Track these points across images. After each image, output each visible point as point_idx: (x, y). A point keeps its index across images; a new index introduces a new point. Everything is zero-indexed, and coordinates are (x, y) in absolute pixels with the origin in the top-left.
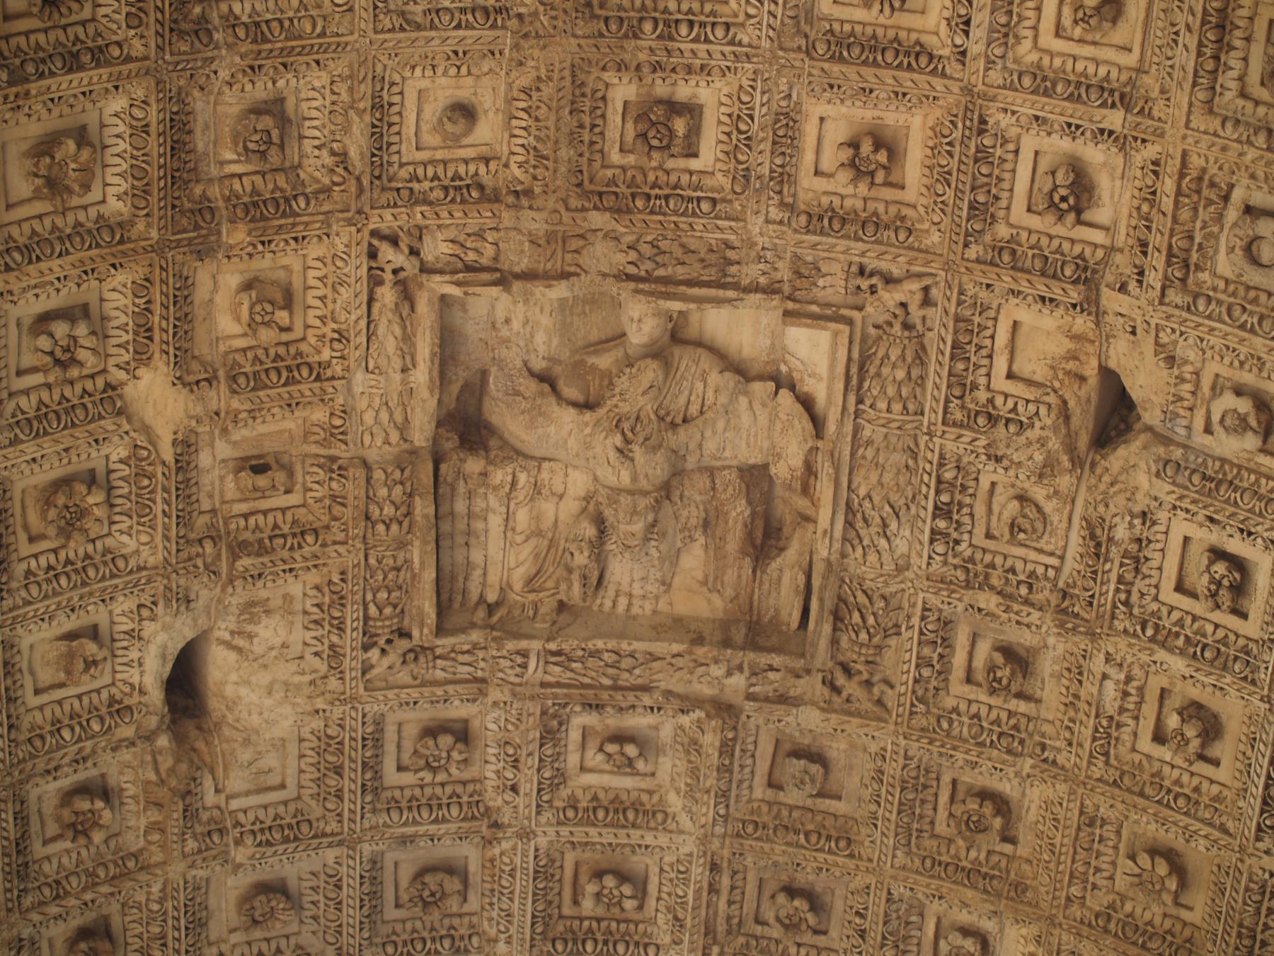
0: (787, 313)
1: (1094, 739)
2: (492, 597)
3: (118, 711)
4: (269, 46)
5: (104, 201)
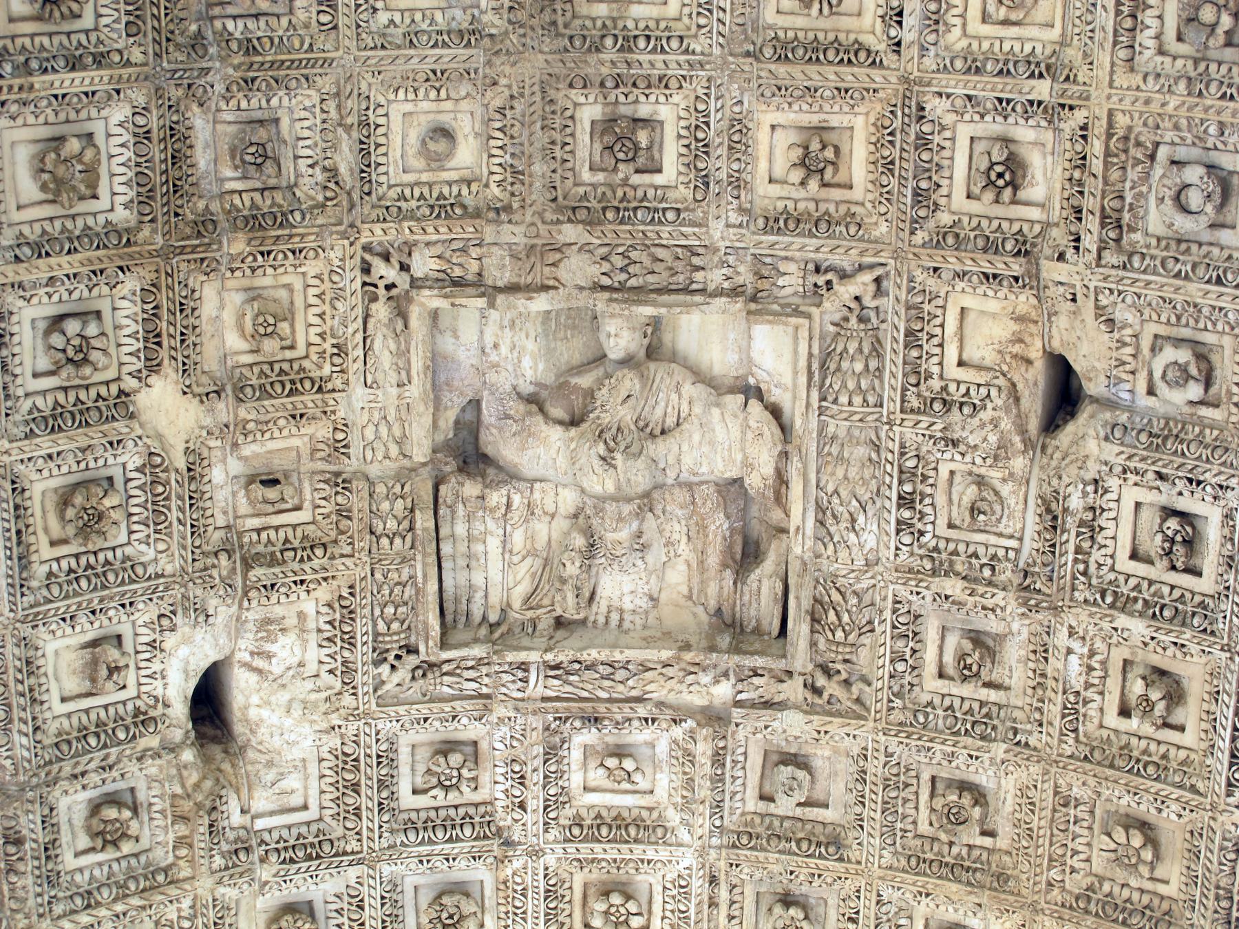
0: (749, 313)
1: (1063, 716)
2: (493, 617)
3: (143, 722)
4: (259, 59)
5: (112, 210)
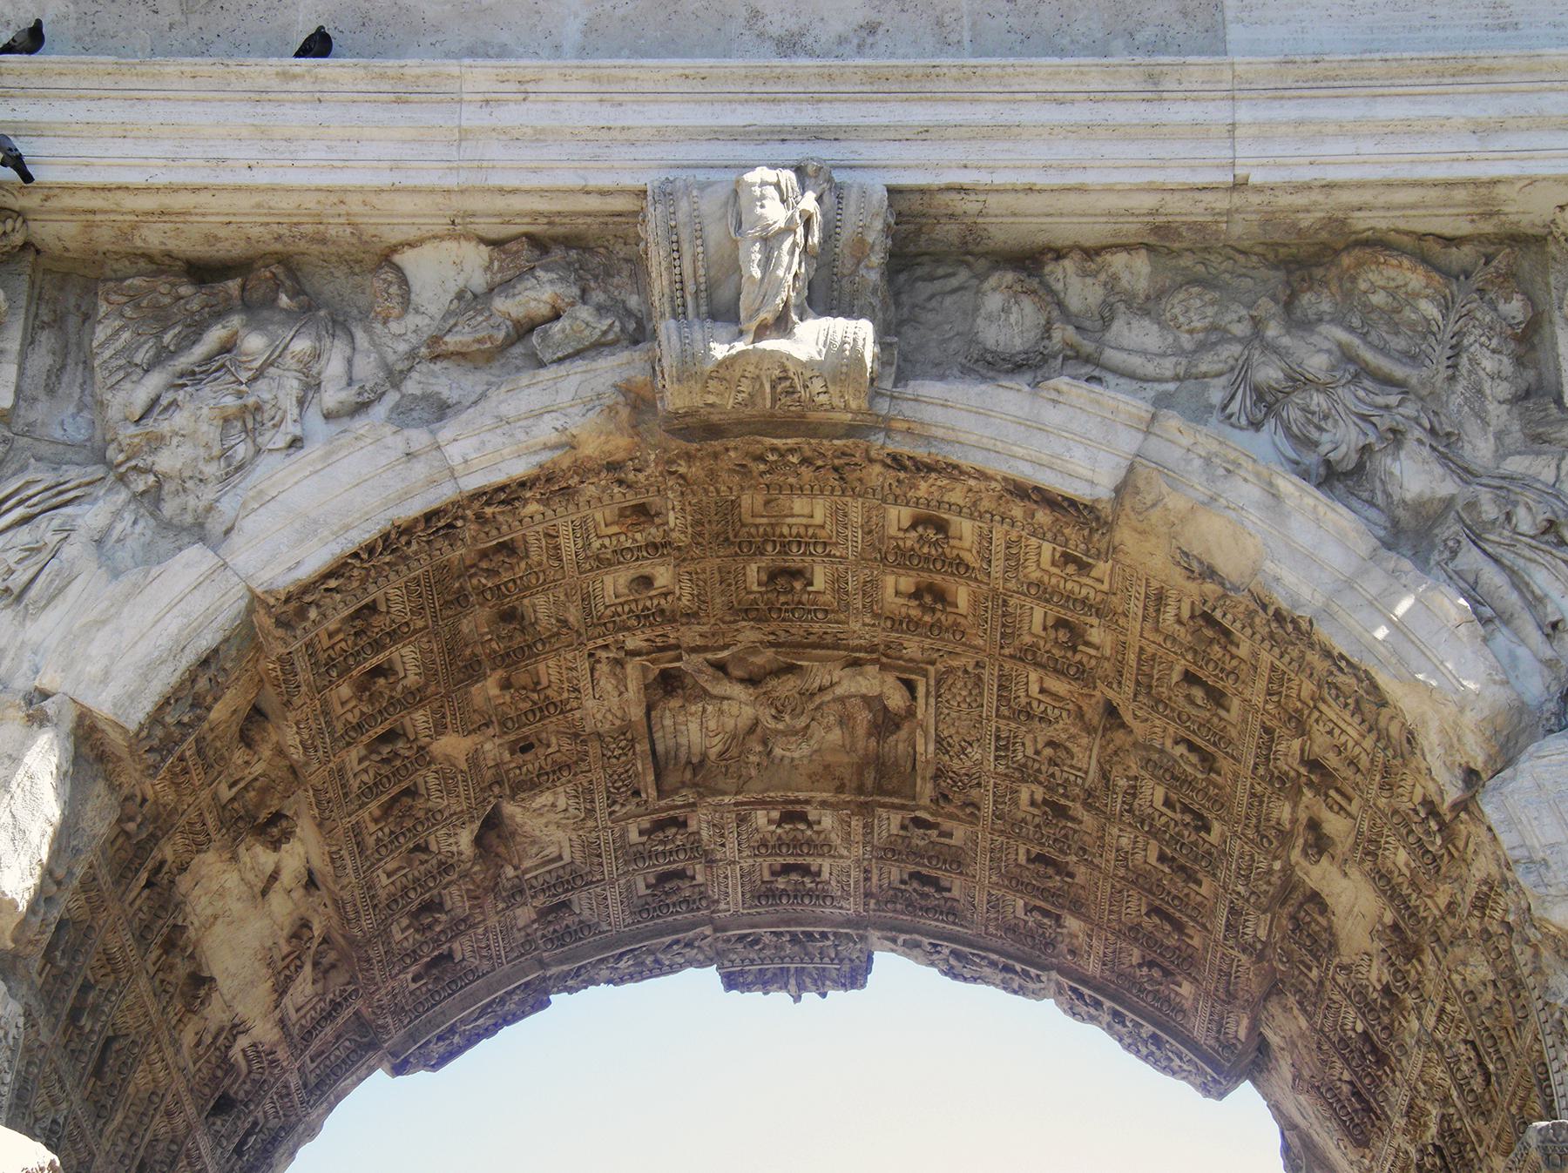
2: (695, 760)
